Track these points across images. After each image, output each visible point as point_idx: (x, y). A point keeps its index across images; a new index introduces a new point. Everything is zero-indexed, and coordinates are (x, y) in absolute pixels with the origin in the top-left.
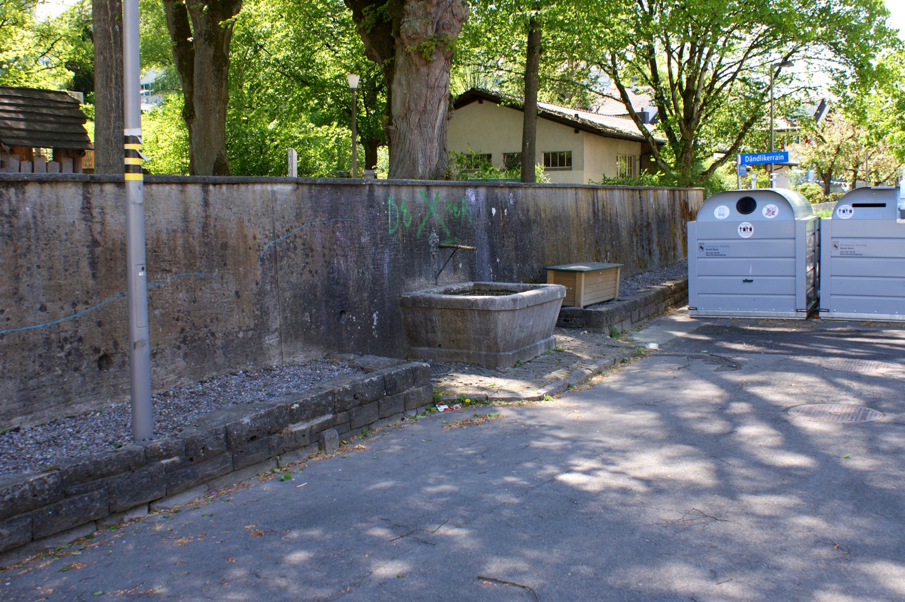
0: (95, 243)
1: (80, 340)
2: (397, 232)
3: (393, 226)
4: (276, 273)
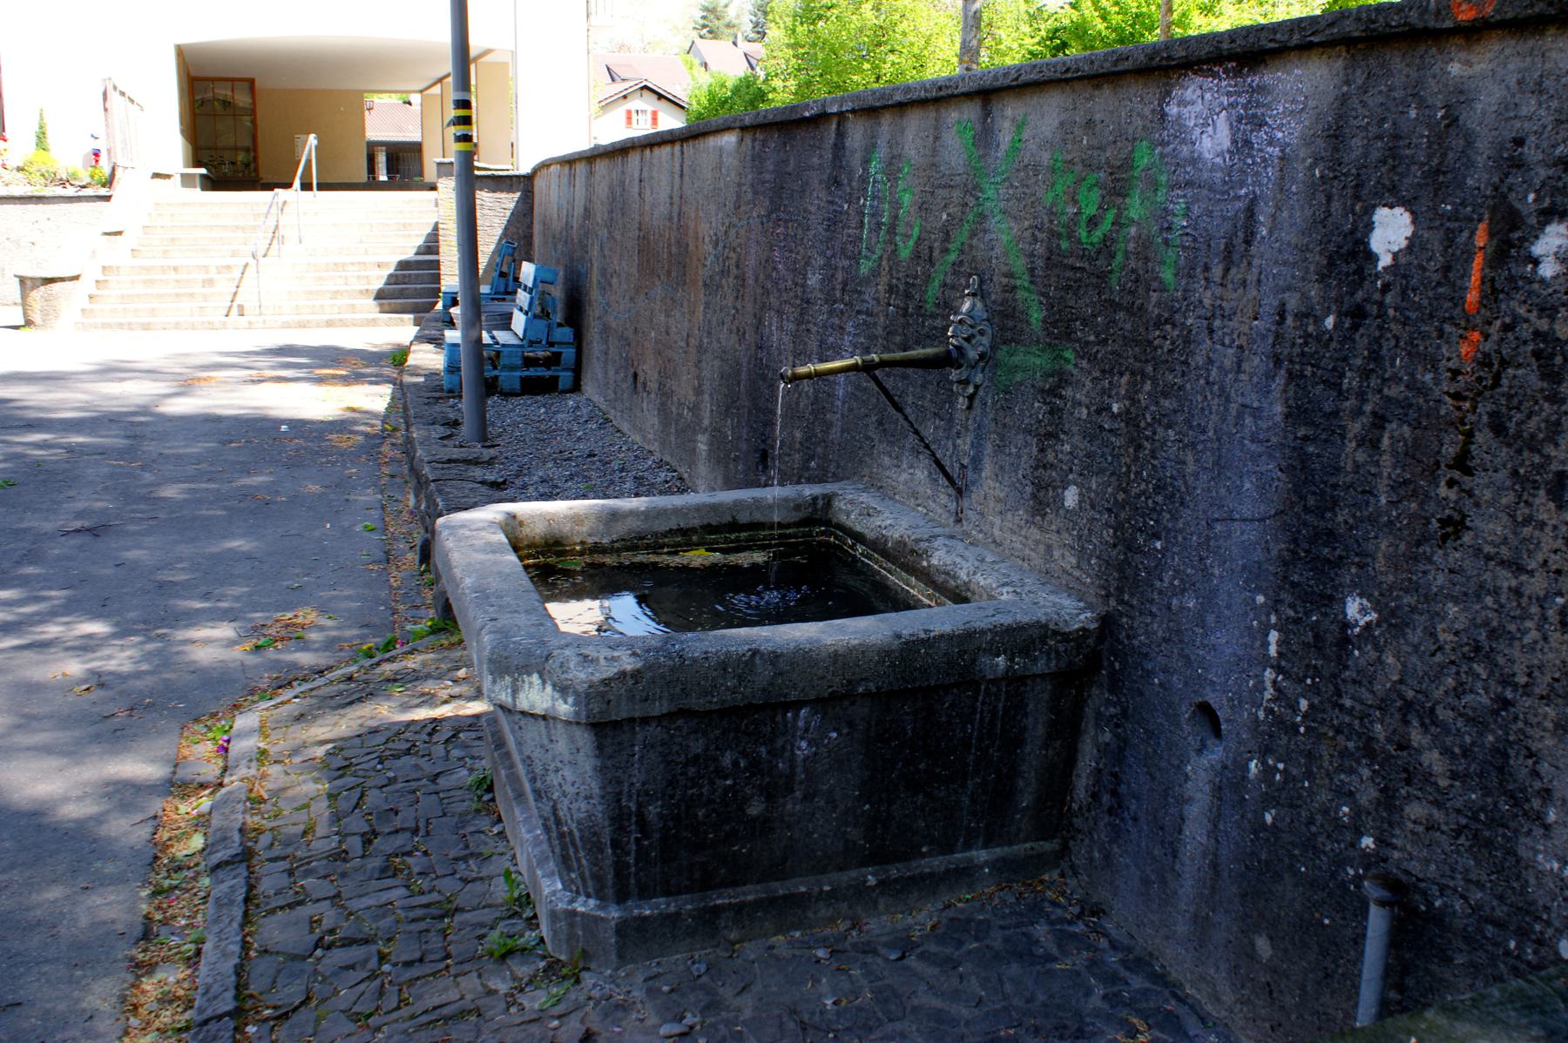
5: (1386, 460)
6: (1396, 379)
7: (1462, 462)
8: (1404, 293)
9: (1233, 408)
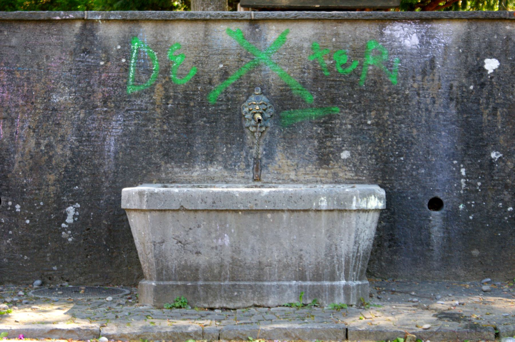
3: (137, 81)
5: (499, 118)
6: (499, 98)
8: (499, 79)
9: (433, 114)
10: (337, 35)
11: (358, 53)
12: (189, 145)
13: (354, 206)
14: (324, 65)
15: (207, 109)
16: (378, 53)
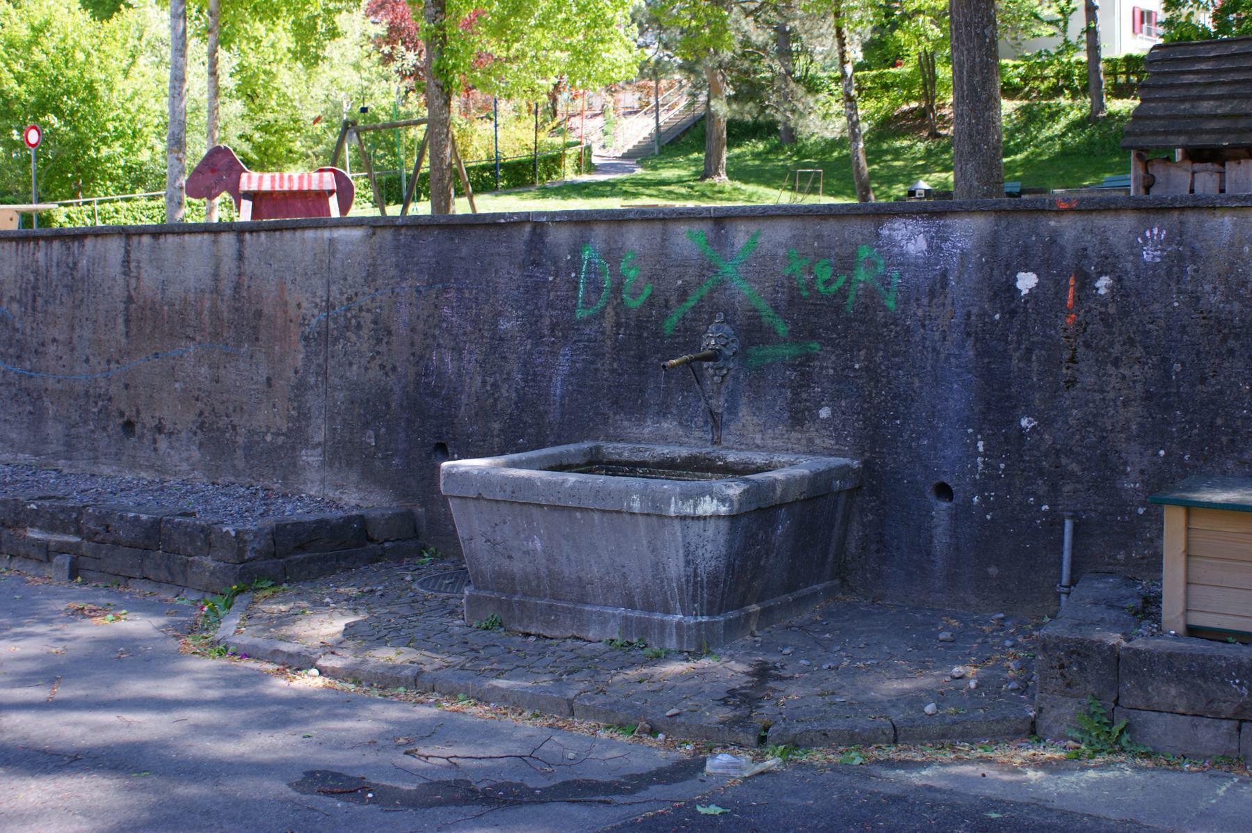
0: (130, 300)
1: (110, 399)
2: (601, 315)
3: (588, 303)
4: (326, 360)
5: (1035, 365)
6: (1036, 334)
7: (1073, 360)
8: (1036, 304)
9: (942, 356)
10: (819, 237)
11: (846, 264)
12: (641, 391)
13: (672, 511)
14: (802, 281)
15: (662, 343)
16: (871, 263)
